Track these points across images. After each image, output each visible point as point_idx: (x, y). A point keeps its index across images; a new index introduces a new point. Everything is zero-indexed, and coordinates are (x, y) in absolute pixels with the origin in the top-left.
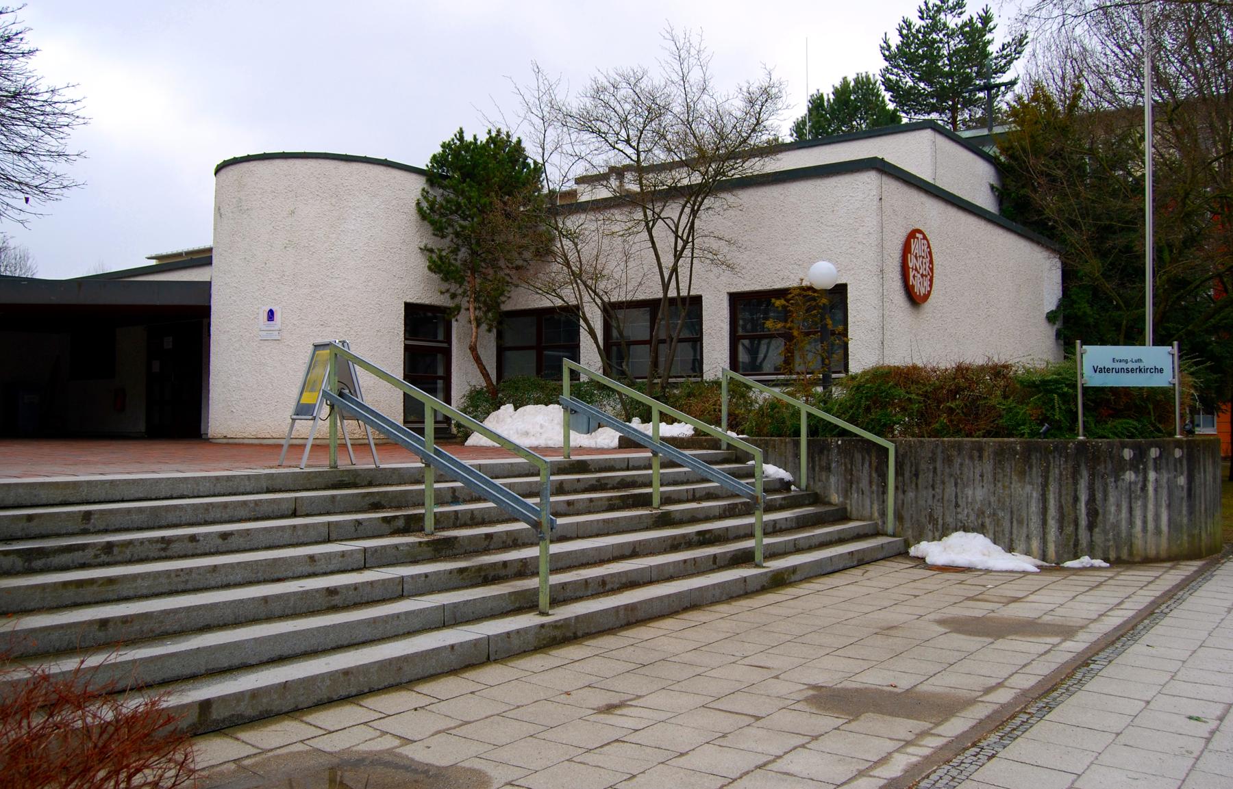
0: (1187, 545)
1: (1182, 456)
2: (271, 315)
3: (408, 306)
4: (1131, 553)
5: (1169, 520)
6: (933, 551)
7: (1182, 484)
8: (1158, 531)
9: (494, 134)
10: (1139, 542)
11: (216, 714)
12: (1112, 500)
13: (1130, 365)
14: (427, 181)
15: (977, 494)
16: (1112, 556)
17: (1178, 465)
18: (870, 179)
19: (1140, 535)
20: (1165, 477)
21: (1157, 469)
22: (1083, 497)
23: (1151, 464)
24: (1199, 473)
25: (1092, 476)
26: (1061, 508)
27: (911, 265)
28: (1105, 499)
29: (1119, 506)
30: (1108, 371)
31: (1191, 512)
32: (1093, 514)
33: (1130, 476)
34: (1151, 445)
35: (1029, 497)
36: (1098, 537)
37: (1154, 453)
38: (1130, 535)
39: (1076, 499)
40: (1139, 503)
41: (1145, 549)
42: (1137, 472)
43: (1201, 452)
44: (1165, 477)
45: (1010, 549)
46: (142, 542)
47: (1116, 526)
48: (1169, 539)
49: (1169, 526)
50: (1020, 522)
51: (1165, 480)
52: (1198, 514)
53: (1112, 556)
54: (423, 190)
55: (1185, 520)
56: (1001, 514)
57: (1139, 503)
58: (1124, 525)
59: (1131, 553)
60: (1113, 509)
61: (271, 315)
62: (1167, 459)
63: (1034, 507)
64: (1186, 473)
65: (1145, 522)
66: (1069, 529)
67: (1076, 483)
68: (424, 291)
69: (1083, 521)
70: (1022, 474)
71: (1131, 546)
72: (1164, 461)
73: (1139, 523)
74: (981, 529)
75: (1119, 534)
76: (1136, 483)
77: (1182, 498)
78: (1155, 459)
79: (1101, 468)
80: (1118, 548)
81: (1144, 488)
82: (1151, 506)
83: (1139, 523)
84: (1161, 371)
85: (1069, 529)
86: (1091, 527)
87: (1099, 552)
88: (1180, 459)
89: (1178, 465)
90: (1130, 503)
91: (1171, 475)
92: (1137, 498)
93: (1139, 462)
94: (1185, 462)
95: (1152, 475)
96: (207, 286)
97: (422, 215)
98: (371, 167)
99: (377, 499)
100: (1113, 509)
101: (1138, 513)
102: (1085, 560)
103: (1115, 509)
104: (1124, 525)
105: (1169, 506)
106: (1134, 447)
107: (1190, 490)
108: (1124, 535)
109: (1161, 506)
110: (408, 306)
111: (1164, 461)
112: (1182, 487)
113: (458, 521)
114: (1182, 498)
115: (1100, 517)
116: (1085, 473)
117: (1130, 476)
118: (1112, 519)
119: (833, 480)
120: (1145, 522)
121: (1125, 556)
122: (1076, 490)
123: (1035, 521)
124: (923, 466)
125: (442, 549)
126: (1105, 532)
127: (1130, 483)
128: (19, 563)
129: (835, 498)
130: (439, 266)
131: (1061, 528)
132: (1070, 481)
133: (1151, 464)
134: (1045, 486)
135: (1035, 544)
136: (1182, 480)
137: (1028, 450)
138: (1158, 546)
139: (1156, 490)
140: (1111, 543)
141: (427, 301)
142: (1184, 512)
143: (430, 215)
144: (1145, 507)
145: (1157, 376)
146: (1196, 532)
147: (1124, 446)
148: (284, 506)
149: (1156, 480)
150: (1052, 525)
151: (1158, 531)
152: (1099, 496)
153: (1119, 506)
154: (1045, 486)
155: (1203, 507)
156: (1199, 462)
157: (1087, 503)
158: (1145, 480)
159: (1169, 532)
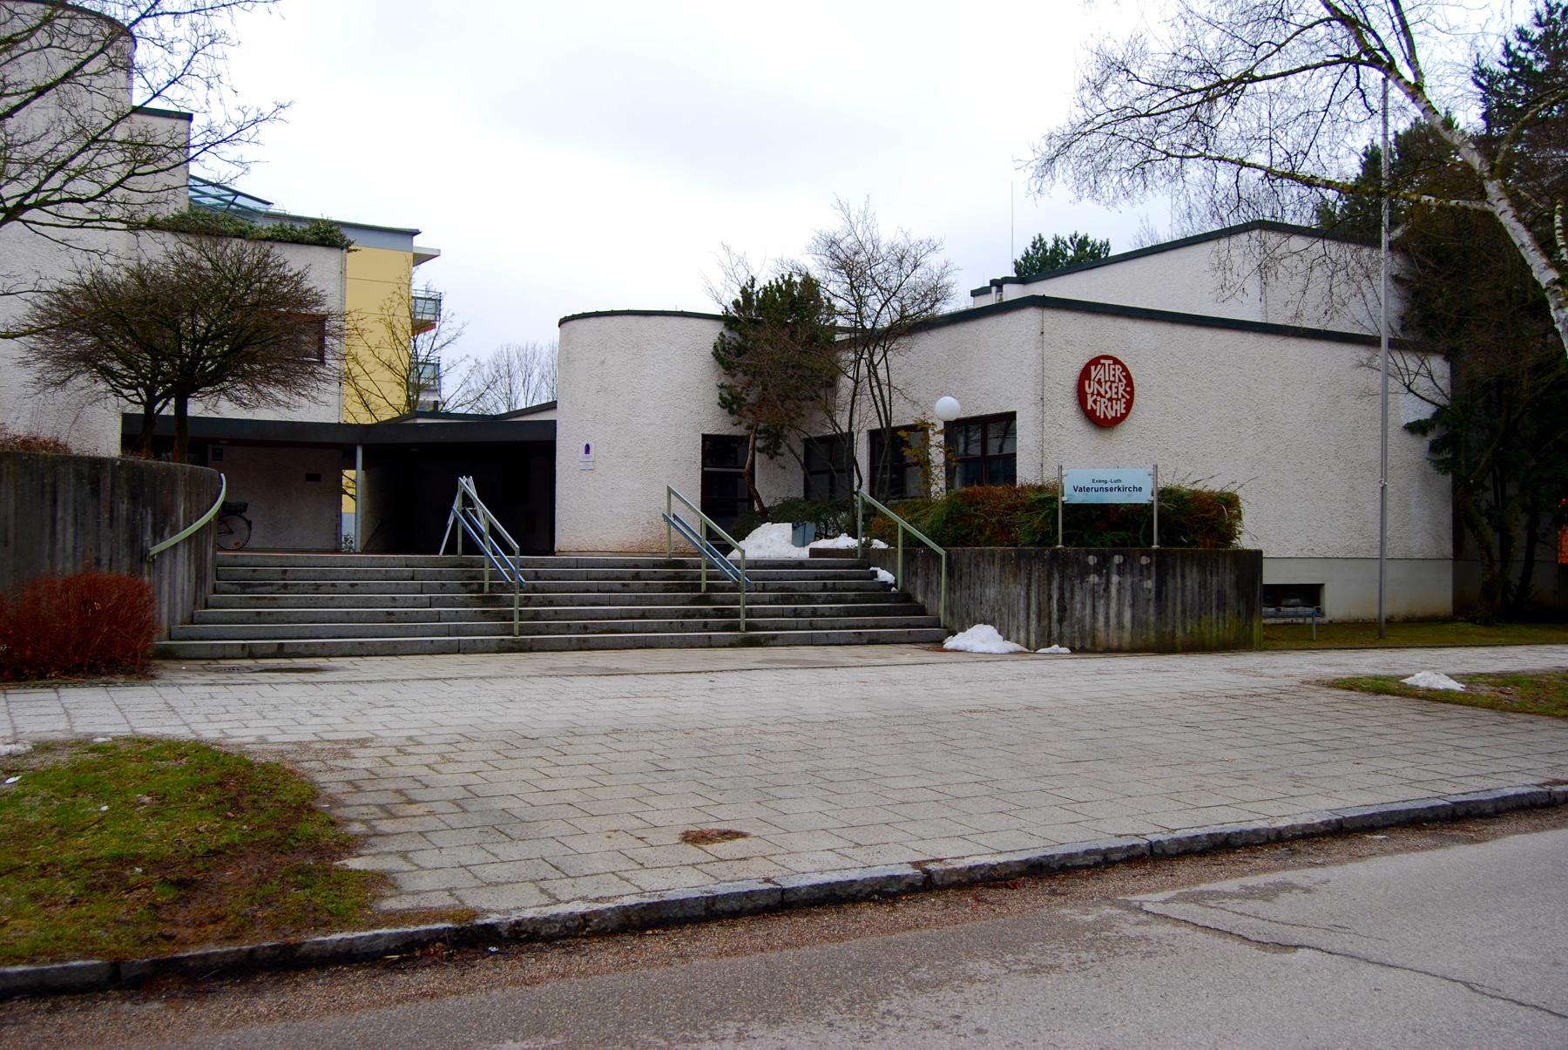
0: (1154, 640)
1: (1151, 563)
2: (587, 448)
3: (705, 438)
4: (1093, 643)
5: (1133, 618)
6: (1039, 651)
7: (1149, 587)
8: (1120, 626)
9: (786, 278)
10: (1101, 635)
11: (286, 650)
12: (1077, 598)
13: (1109, 485)
14: (726, 325)
15: (991, 592)
16: (1078, 645)
17: (1145, 571)
18: (1030, 316)
19: (1102, 629)
20: (1128, 581)
21: (1119, 574)
22: (1055, 596)
23: (1114, 569)
24: (1174, 576)
25: (1062, 578)
26: (1039, 604)
27: (1088, 391)
28: (1072, 598)
29: (1083, 604)
30: (1088, 489)
31: (1161, 611)
32: (1062, 609)
33: (1093, 579)
34: (1115, 553)
35: (1019, 595)
36: (1066, 630)
37: (1117, 559)
38: (1093, 628)
39: (1050, 597)
40: (1102, 602)
41: (1108, 641)
42: (1100, 575)
43: (1179, 562)
44: (1128, 581)
45: (1007, 638)
46: (304, 585)
47: (1081, 620)
48: (1132, 634)
49: (1133, 623)
50: (1014, 616)
51: (1129, 583)
52: (1170, 614)
53: (1078, 645)
54: (721, 334)
55: (1152, 619)
56: (1003, 609)
57: (1102, 602)
58: (1088, 620)
59: (1093, 643)
60: (1078, 606)
61: (587, 448)
62: (1132, 565)
63: (1022, 604)
64: (1154, 578)
65: (1107, 618)
66: (1045, 622)
67: (1050, 584)
68: (720, 424)
69: (1055, 617)
70: (1015, 576)
71: (1094, 637)
72: (1128, 566)
73: (1101, 619)
74: (992, 622)
75: (1083, 626)
76: (1099, 585)
77: (1149, 600)
78: (1119, 565)
79: (1069, 571)
80: (1082, 639)
81: (1107, 589)
82: (1113, 605)
83: (1101, 619)
84: (1140, 489)
85: (1045, 622)
86: (1061, 621)
87: (1066, 642)
88: (1148, 566)
89: (1145, 571)
90: (1093, 601)
91: (1136, 579)
92: (1100, 598)
93: (1103, 567)
94: (1153, 569)
95: (1115, 579)
96: (552, 424)
97: (716, 354)
98: (667, 318)
99: (474, 574)
100: (1078, 606)
101: (1101, 611)
102: (1055, 647)
103: (1080, 607)
104: (1088, 620)
105: (1133, 606)
106: (1096, 554)
107: (1159, 594)
108: (1088, 628)
109: (1124, 605)
110: (705, 438)
111: (1128, 566)
112: (1150, 591)
113: (534, 589)
114: (1149, 600)
115: (1068, 612)
116: (1057, 576)
117: (1093, 579)
118: (1077, 614)
119: (919, 582)
120: (1107, 618)
121: (1088, 646)
122: (1050, 590)
123: (1022, 613)
124: (964, 570)
125: (486, 601)
126: (1072, 626)
127: (1094, 585)
128: (239, 589)
129: (920, 598)
130: (730, 402)
131: (1039, 621)
132: (1046, 582)
133: (1114, 569)
134: (1029, 585)
135: (1022, 634)
136: (1149, 584)
137: (1020, 555)
138: (1120, 639)
139: (1119, 592)
140: (1077, 635)
141: (726, 433)
142: (1152, 610)
143: (725, 356)
144: (1108, 606)
145: (1136, 494)
146: (1169, 629)
147: (1089, 553)
148: (406, 574)
149: (1119, 583)
150: (1033, 616)
151: (1120, 626)
152: (1067, 595)
153: (1083, 604)
154: (1029, 585)
155: (1179, 609)
156: (1174, 569)
157: (1058, 601)
158: (1108, 582)
159: (1133, 627)
